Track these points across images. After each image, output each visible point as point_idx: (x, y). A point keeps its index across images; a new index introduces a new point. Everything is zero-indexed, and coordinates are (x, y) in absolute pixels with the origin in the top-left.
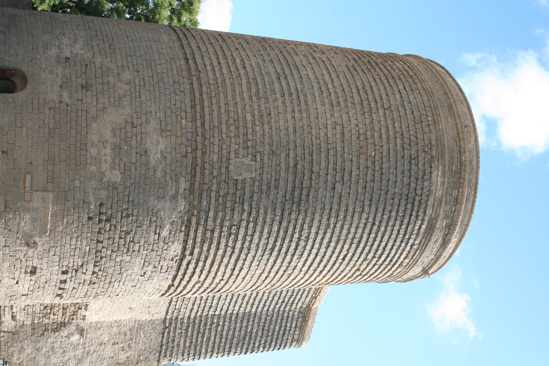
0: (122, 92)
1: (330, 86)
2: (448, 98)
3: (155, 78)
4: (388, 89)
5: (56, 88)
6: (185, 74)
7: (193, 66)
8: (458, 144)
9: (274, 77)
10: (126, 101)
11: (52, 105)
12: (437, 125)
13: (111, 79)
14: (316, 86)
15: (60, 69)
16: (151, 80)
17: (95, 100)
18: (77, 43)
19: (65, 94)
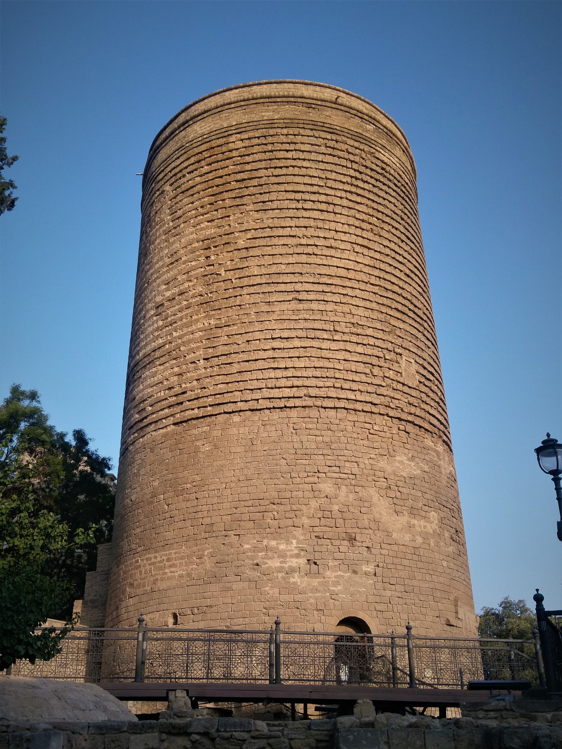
0: (351, 497)
1: (304, 241)
2: (295, 102)
3: (325, 452)
4: (296, 171)
5: (357, 578)
6: (314, 413)
7: (298, 402)
8: (353, 116)
9: (294, 305)
10: (363, 493)
11: (379, 585)
12: (335, 131)
13: (335, 508)
14: (304, 258)
15: (328, 573)
16: (329, 457)
17: (367, 531)
18: (278, 548)
19: (365, 568)
